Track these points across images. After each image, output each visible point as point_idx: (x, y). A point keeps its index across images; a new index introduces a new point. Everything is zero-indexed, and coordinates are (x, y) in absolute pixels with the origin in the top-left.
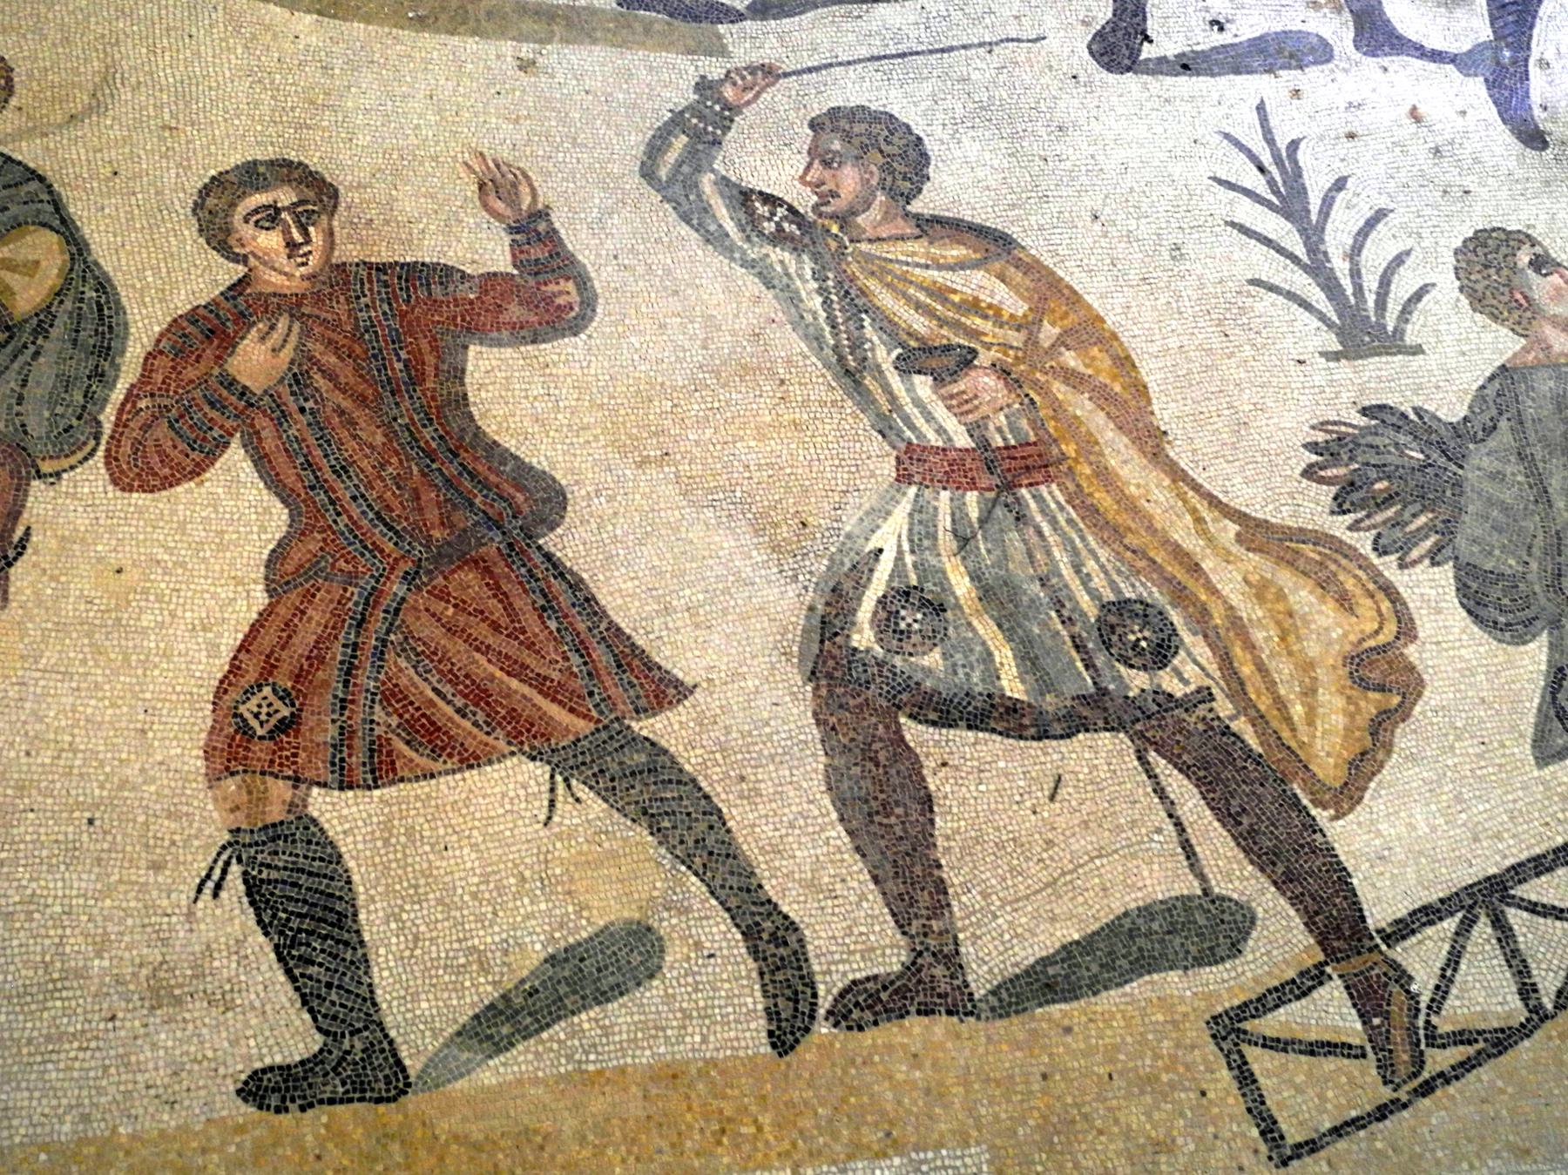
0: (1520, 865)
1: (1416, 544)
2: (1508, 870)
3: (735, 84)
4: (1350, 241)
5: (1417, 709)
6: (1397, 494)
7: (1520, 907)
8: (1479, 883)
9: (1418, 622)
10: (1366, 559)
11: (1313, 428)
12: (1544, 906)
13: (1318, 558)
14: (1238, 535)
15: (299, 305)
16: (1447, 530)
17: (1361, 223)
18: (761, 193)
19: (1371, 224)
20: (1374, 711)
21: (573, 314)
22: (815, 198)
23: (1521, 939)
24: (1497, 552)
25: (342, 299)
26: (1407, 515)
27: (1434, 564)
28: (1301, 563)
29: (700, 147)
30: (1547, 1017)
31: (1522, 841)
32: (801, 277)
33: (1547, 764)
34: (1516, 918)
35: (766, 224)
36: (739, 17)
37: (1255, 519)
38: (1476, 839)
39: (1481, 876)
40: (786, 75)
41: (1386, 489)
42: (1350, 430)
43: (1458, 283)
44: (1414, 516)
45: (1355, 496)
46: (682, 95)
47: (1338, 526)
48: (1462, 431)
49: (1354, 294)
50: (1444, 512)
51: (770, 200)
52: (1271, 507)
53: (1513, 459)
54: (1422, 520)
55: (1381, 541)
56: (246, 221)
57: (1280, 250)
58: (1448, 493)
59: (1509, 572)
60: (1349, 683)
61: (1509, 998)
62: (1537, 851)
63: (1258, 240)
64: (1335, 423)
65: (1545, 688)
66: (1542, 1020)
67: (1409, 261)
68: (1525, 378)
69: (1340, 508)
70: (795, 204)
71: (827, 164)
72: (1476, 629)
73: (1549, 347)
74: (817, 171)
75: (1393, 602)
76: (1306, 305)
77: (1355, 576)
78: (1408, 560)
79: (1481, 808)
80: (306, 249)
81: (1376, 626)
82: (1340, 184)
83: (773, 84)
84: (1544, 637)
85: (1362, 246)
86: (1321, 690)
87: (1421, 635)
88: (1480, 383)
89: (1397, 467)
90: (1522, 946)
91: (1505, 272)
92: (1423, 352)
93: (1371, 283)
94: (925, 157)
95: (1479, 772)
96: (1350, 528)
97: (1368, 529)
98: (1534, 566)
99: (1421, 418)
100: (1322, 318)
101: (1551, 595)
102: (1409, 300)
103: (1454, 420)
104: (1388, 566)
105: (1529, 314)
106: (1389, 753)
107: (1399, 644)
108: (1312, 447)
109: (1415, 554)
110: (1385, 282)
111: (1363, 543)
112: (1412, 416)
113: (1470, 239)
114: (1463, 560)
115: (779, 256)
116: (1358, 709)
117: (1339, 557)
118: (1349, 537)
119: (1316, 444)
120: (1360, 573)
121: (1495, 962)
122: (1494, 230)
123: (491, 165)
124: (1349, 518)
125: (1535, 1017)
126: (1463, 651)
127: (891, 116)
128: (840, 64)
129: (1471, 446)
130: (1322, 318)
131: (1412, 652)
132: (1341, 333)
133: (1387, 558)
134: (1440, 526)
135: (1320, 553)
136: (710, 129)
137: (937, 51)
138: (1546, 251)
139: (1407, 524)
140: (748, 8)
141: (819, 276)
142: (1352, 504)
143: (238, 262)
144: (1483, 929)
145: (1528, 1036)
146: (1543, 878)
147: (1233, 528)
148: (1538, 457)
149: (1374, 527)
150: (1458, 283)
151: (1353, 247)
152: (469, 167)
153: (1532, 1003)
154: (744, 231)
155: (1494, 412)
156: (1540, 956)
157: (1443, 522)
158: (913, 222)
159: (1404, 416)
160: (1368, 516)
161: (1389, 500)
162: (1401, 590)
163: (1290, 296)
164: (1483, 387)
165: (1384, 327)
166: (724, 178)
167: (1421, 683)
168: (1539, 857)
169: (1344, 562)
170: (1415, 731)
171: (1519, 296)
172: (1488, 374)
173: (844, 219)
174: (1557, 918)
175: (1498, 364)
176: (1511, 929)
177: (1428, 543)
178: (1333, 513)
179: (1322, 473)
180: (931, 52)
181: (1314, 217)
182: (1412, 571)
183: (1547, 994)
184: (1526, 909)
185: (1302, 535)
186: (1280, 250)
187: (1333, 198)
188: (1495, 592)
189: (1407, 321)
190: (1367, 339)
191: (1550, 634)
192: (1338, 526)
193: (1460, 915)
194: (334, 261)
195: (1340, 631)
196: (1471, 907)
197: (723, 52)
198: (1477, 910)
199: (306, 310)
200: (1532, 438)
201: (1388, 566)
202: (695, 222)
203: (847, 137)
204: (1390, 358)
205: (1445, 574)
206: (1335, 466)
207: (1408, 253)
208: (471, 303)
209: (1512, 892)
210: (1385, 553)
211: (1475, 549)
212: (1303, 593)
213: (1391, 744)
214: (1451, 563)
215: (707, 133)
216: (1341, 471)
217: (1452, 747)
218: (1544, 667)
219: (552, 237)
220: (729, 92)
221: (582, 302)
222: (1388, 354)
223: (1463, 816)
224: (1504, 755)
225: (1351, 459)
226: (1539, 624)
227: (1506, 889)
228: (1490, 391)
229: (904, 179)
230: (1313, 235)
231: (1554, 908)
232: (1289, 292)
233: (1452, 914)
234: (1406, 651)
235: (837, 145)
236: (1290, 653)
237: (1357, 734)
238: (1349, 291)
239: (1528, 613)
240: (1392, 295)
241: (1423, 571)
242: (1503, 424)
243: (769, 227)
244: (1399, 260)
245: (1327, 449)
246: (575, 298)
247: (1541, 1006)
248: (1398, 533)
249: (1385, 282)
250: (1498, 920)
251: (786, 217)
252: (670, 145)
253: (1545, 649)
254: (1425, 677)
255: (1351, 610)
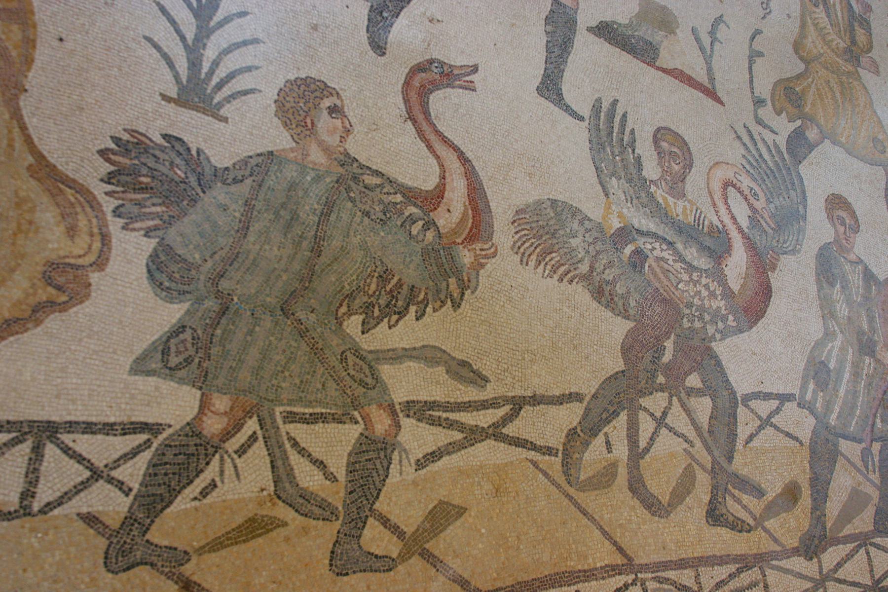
0: (76, 423)
1: (142, 220)
2: (66, 423)
4: (225, 46)
5: (75, 309)
6: (152, 188)
7: (58, 446)
8: (41, 422)
9: (111, 263)
10: (104, 214)
11: (125, 130)
12: (74, 452)
13: (73, 199)
14: (31, 165)
16: (168, 223)
17: (239, 40)
19: (245, 43)
20: (44, 299)
23: (45, 464)
24: (191, 247)
26: (148, 203)
27: (146, 235)
28: (59, 199)
30: (29, 514)
31: (87, 410)
33: (136, 374)
34: (51, 450)
37: (48, 161)
38: (58, 396)
39: (46, 418)
41: (148, 183)
42: (148, 142)
43: (276, 97)
44: (154, 205)
45: (123, 178)
47: (99, 190)
48: (220, 173)
49: (206, 74)
50: (174, 211)
52: (64, 159)
53: (240, 202)
54: (159, 209)
55: (122, 209)
57: (178, 31)
58: (185, 203)
59: (191, 260)
60: (40, 276)
61: (12, 494)
62: (94, 419)
63: (168, 19)
64: (141, 134)
65: (166, 333)
66: (25, 515)
67: (254, 73)
68: (280, 163)
69: (108, 179)
72: (146, 282)
73: (308, 155)
75: (103, 245)
76: (171, 65)
77: (89, 221)
78: (131, 226)
79: (74, 381)
81: (82, 252)
82: (243, 14)
84: (186, 305)
85: (231, 51)
86: (18, 273)
87: (108, 270)
88: (250, 154)
89: (163, 174)
90: (43, 468)
91: (311, 105)
92: (227, 122)
93: (221, 72)
95: (88, 361)
96: (106, 193)
97: (116, 199)
98: (210, 264)
99: (199, 155)
100: (177, 77)
101: (209, 285)
102: (239, 92)
103: (219, 166)
104: (115, 225)
105: (308, 133)
106: (37, 325)
107: (89, 269)
108: (116, 140)
109: (137, 225)
110: (231, 76)
111: (109, 205)
112: (194, 152)
113: (302, 79)
114: (166, 242)
116: (35, 294)
117: (86, 205)
118: (102, 198)
119: (120, 139)
120: (94, 221)
121: (18, 470)
122: (319, 81)
124: (110, 188)
125: (22, 511)
126: (128, 290)
129: (219, 184)
130: (177, 77)
131: (94, 277)
132: (182, 89)
133: (118, 219)
134: (166, 217)
135: (76, 198)
138: (343, 106)
139: (145, 207)
142: (119, 181)
144: (26, 447)
145: (9, 520)
146: (86, 436)
147: (30, 159)
148: (257, 208)
149: (123, 199)
150: (276, 97)
151: (225, 50)
153: (25, 503)
155: (247, 173)
156: (51, 478)
157: (170, 216)
159: (189, 149)
160: (123, 192)
161: (144, 189)
162: (114, 240)
163: (166, 57)
164: (251, 157)
165: (212, 99)
167: (88, 296)
168: (92, 423)
169: (88, 209)
170: (63, 321)
171: (309, 121)
172: (259, 151)
174: (79, 462)
175: (270, 149)
176: (43, 456)
177: (151, 223)
178: (102, 180)
179: (112, 157)
181: (212, 24)
182: (129, 233)
183: (39, 501)
184: (62, 449)
185: (71, 183)
186: (178, 31)
187: (232, 19)
188: (174, 267)
189: (229, 102)
190: (196, 100)
191: (192, 305)
192: (99, 190)
193: (14, 435)
195: (56, 245)
196: (26, 433)
198: (29, 436)
200: (260, 197)
201: (115, 225)
204: (203, 116)
205: (150, 245)
206: (123, 156)
207: (257, 68)
209: (59, 436)
210: (119, 216)
211: (179, 239)
212: (48, 215)
213: (42, 322)
214: (157, 240)
216: (128, 162)
217: (81, 340)
218: (174, 321)
222: (204, 113)
223: (59, 380)
224: (111, 358)
225: (136, 157)
226: (188, 296)
227: (56, 432)
228: (253, 162)
230: (204, 33)
231: (80, 455)
232: (165, 54)
233: (9, 432)
234: (91, 275)
236: (14, 244)
237: (24, 307)
238: (205, 70)
239: (186, 288)
240: (230, 85)
241: (136, 238)
242: (248, 181)
244: (249, 69)
245: (125, 145)
247: (30, 507)
248: (135, 210)
249: (231, 76)
250: (38, 447)
253: (182, 312)
254: (93, 294)
255: (72, 238)
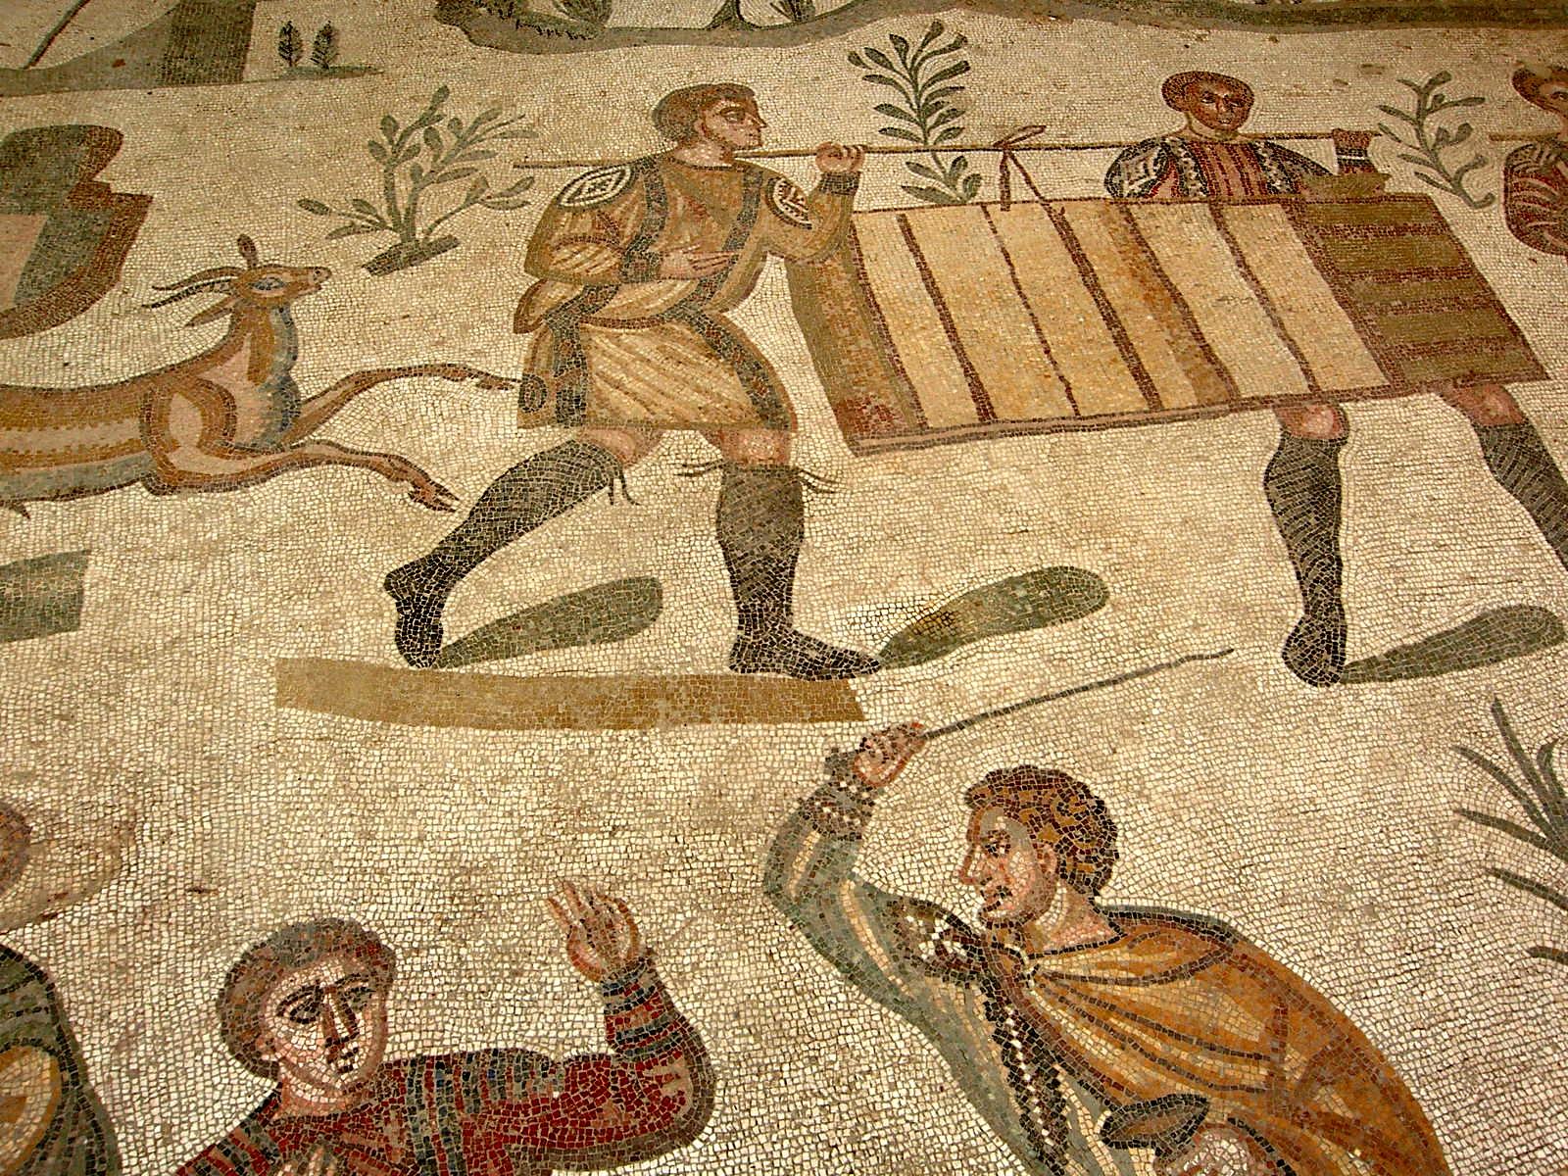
3: (873, 755)
15: (339, 1129)
18: (914, 902)
21: (685, 1109)
22: (981, 900)
25: (393, 1115)
29: (836, 845)
32: (971, 1015)
35: (922, 946)
36: (875, 666)
40: (933, 735)
46: (812, 779)
51: (926, 910)
56: (280, 1014)
70: (957, 912)
71: (991, 851)
74: (980, 863)
80: (352, 1046)
83: (920, 748)
94: (1110, 826)
115: (946, 990)
123: (583, 900)
127: (1063, 775)
128: (996, 713)
136: (846, 819)
137: (1108, 683)
140: (882, 654)
141: (994, 1013)
143: (266, 1075)
152: (556, 905)
154: (896, 958)
158: (1104, 921)
166: (867, 885)
173: (1021, 926)
180: (1101, 685)
194: (385, 1059)
197: (856, 714)
199: (346, 1138)
202: (834, 953)
203: (1013, 811)
208: (555, 1105)
215: (843, 825)
219: (655, 997)
220: (866, 768)
221: (696, 1089)
229: (1088, 860)
235: (1001, 824)
243: (927, 950)
246: (687, 1085)
251: (947, 931)
252: (800, 847)
